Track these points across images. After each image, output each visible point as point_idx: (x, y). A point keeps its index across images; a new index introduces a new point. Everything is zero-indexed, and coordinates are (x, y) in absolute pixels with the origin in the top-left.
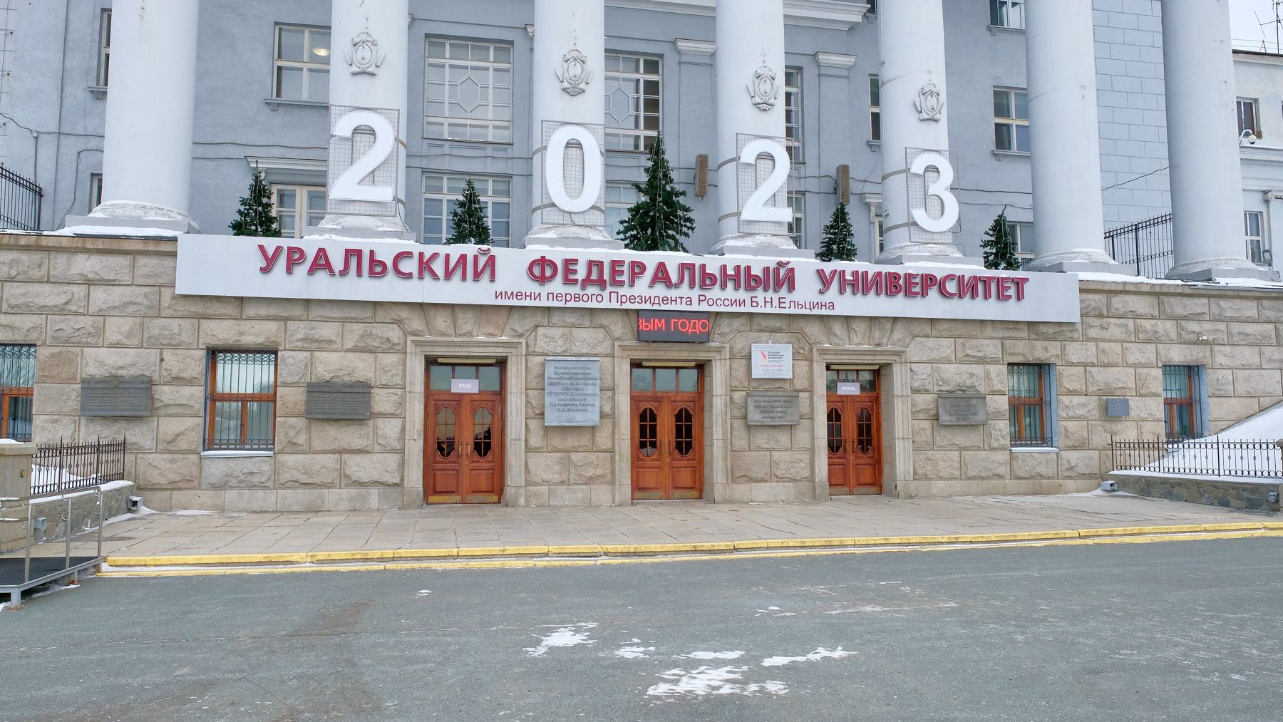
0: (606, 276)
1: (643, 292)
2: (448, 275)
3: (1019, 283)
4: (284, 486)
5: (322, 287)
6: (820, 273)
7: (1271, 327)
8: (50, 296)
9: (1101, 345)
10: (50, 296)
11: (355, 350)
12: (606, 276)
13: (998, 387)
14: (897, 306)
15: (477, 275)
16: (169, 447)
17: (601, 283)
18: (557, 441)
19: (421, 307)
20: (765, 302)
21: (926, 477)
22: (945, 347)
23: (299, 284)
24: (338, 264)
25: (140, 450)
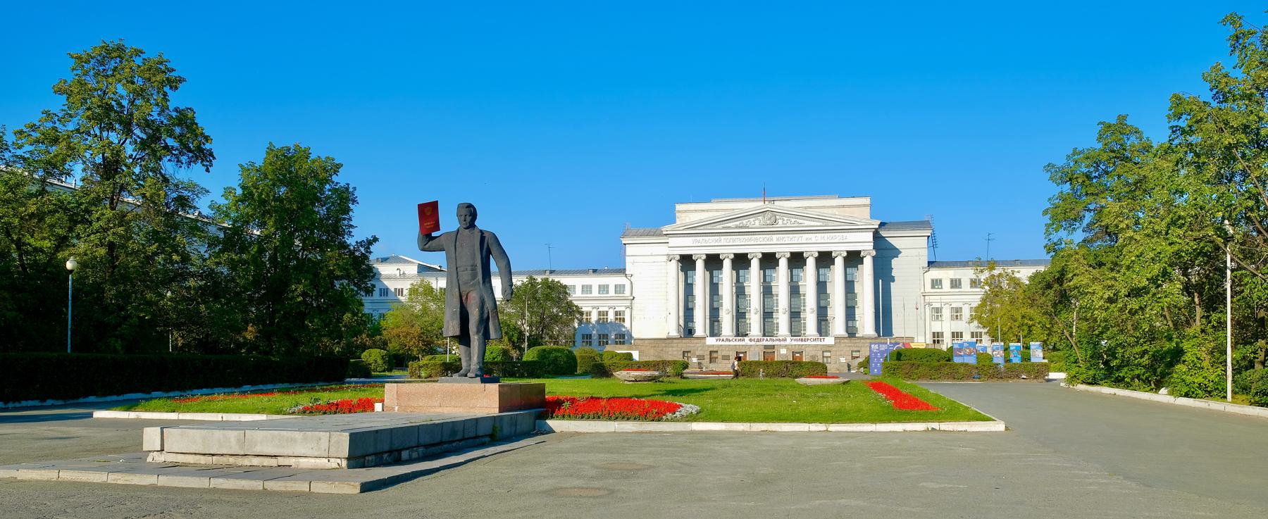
1: (765, 343)
5: (723, 343)
10: (692, 345)
14: (803, 343)
20: (782, 343)
22: (811, 349)
23: (721, 343)
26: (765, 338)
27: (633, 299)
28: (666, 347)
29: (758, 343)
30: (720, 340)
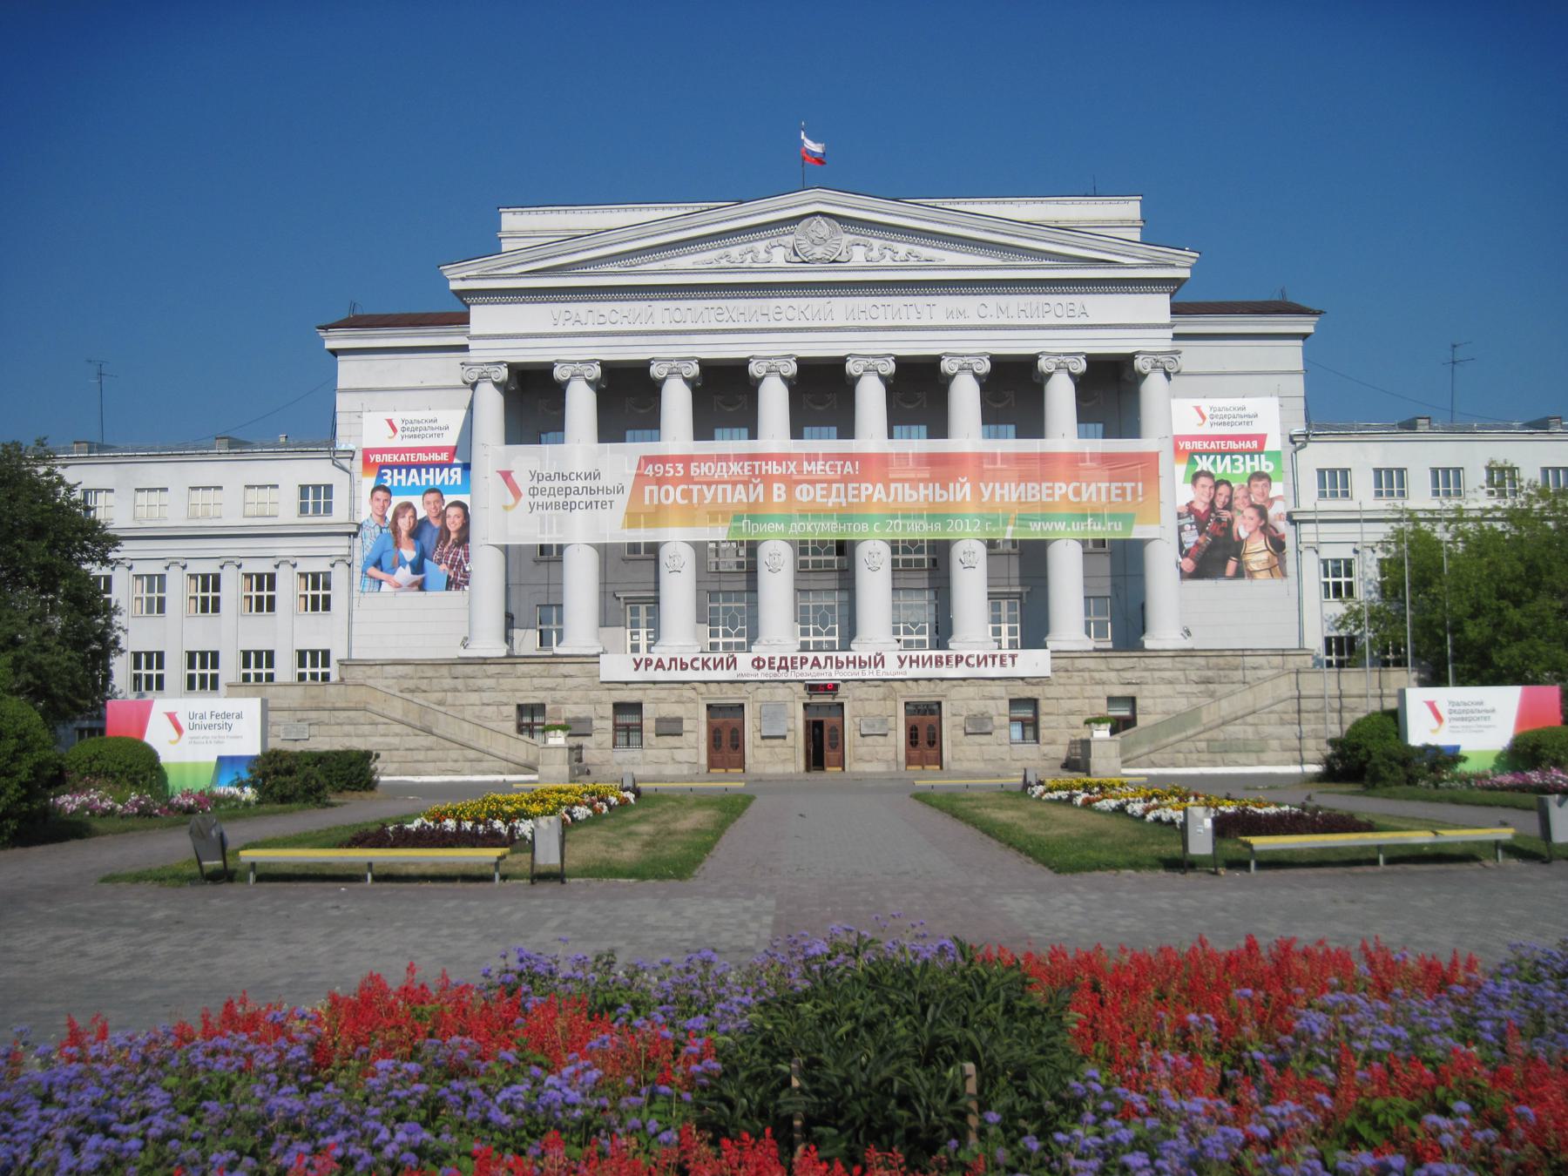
0: (789, 664)
2: (715, 667)
3: (1013, 657)
4: (647, 764)
5: (660, 675)
6: (899, 657)
7: (1179, 673)
8: (549, 682)
9: (1069, 688)
10: (549, 682)
11: (677, 702)
12: (789, 664)
13: (1002, 712)
15: (728, 667)
16: (599, 746)
17: (786, 668)
18: (768, 742)
19: (705, 682)
20: (869, 673)
21: (959, 760)
22: (969, 691)
24: (667, 666)
25: (588, 748)
26: (810, 656)
27: (355, 535)
28: (455, 690)
29: (783, 675)
30: (648, 663)
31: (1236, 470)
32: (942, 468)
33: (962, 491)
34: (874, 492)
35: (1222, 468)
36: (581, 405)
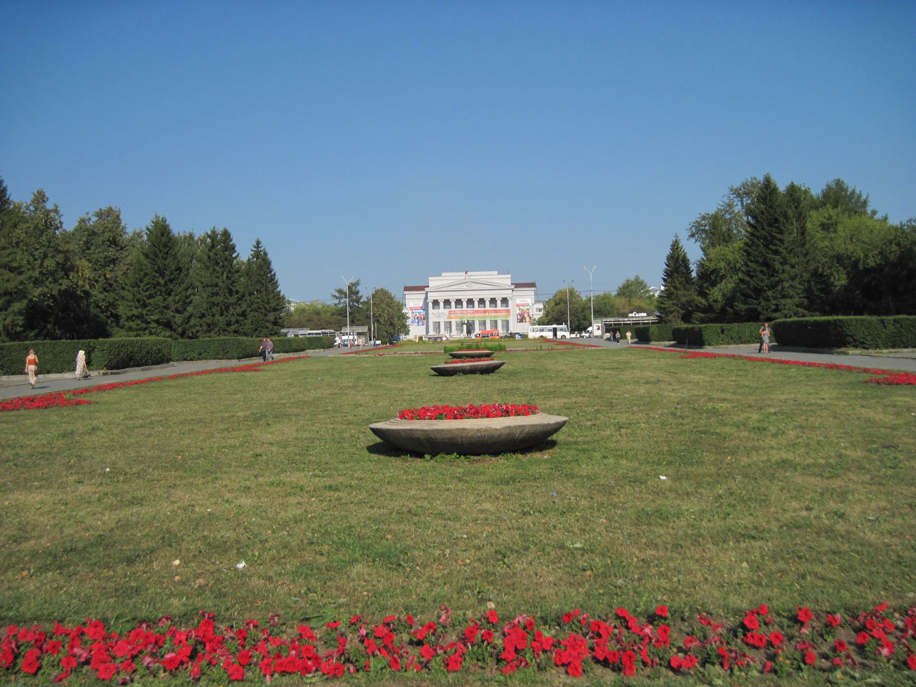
31: (525, 308)
32: (485, 312)
33: (487, 314)
34: (476, 315)
35: (523, 308)
36: (442, 304)
